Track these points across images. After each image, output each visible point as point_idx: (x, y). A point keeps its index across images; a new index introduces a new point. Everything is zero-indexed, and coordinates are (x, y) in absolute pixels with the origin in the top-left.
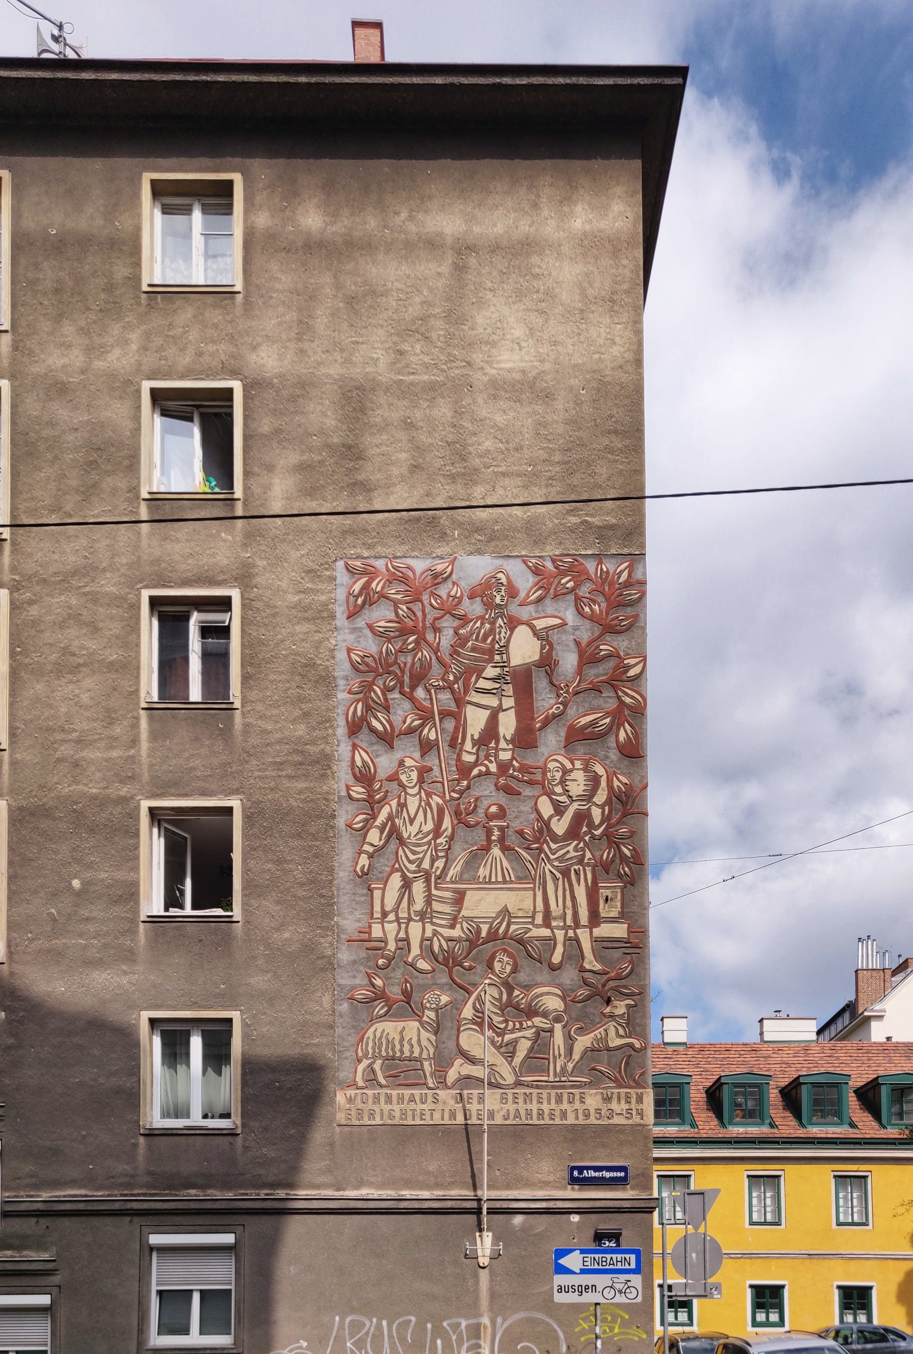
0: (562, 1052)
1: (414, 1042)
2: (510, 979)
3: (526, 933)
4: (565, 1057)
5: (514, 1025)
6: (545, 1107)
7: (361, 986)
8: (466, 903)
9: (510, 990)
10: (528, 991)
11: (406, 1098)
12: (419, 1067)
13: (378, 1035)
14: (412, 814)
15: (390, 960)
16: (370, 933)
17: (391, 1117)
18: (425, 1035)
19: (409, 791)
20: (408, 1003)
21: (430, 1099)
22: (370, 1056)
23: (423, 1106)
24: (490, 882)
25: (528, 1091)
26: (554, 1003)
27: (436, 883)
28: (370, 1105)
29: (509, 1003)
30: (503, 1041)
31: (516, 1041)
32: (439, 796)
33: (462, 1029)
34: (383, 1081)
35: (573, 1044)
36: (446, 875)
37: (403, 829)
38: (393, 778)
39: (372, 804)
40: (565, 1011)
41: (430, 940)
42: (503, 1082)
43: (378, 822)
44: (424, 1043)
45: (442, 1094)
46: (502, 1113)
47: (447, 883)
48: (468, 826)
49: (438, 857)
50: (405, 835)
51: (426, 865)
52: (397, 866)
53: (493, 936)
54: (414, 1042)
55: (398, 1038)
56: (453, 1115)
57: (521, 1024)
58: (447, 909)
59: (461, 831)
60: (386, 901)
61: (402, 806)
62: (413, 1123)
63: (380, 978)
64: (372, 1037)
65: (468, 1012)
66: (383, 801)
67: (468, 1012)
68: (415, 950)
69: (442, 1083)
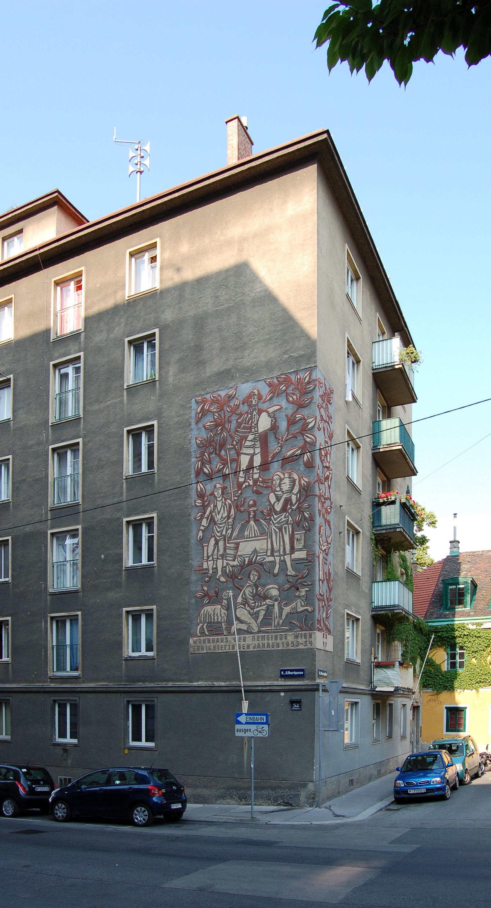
3: (263, 560)
6: (270, 642)
9: (257, 587)
11: (216, 640)
15: (210, 578)
16: (202, 566)
17: (210, 649)
18: (223, 611)
19: (219, 499)
21: (225, 640)
24: (249, 538)
26: (275, 592)
27: (228, 541)
38: (212, 494)
39: (204, 507)
40: (279, 596)
41: (226, 567)
43: (206, 516)
44: (223, 615)
46: (253, 645)
49: (229, 528)
51: (224, 533)
53: (250, 563)
54: (219, 614)
55: (212, 613)
58: (232, 552)
61: (215, 506)
65: (240, 600)
66: (208, 505)
67: (240, 600)
68: (220, 573)
69: (230, 633)
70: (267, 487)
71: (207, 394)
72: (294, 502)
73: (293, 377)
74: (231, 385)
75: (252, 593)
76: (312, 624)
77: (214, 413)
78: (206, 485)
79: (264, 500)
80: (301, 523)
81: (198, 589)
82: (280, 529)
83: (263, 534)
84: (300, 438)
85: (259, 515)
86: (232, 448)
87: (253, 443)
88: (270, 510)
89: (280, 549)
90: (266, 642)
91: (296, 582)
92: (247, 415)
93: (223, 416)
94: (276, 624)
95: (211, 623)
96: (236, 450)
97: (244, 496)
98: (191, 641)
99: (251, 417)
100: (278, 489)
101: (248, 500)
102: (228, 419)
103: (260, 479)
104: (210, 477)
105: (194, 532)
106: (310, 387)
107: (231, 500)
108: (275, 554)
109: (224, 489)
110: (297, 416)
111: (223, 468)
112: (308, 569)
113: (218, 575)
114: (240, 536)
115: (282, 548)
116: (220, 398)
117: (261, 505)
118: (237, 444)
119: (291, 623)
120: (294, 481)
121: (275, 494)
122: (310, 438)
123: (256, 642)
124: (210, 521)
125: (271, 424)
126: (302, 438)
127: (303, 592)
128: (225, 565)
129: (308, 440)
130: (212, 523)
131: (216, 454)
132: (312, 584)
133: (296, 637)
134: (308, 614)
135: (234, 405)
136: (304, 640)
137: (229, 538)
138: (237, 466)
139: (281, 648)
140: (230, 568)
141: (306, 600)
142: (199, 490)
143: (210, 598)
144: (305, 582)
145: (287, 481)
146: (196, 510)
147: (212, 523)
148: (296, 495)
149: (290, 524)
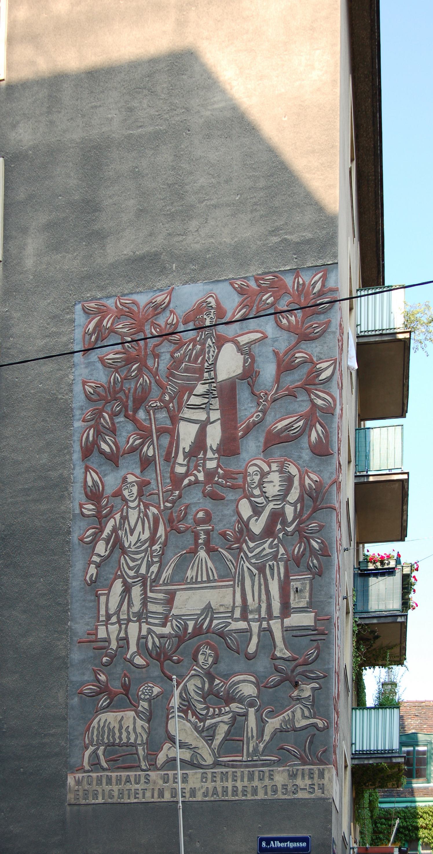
0: (255, 734)
2: (211, 670)
3: (226, 626)
4: (257, 739)
7: (88, 681)
8: (176, 603)
10: (227, 679)
11: (124, 779)
12: (135, 752)
13: (102, 724)
14: (132, 524)
15: (112, 657)
16: (96, 634)
17: (111, 796)
18: (140, 723)
19: (131, 505)
20: (127, 695)
21: (143, 780)
22: (95, 743)
23: (137, 786)
24: (196, 582)
25: (224, 770)
26: (249, 690)
27: (151, 586)
28: (95, 787)
29: (210, 692)
30: (204, 725)
32: (155, 507)
33: (170, 716)
34: (105, 765)
35: (264, 726)
37: (125, 539)
38: (118, 494)
39: (100, 519)
40: (258, 697)
41: (146, 637)
43: (104, 536)
44: (139, 730)
45: (153, 775)
47: (161, 585)
49: (153, 563)
50: (126, 545)
51: (143, 570)
52: (119, 573)
53: (198, 631)
55: (117, 726)
56: (161, 794)
57: (220, 710)
58: (159, 609)
59: (173, 538)
61: (125, 518)
62: (129, 801)
63: (104, 674)
64: (96, 726)
65: (175, 702)
66: (110, 515)
67: (175, 702)
68: (133, 648)
69: (153, 766)
70: (233, 487)
71: (108, 297)
72: (290, 518)
73: (289, 280)
74: (159, 285)
75: (202, 689)
76: (324, 752)
78: (105, 475)
79: (229, 511)
80: (303, 560)
81: (86, 678)
82: (261, 569)
83: (224, 577)
84: (302, 397)
85: (216, 541)
86: (161, 408)
87: (206, 401)
88: (241, 531)
89: (260, 606)
90: (229, 784)
91: (293, 671)
92: (194, 346)
94: (251, 749)
95: (113, 745)
96: (168, 411)
97: (186, 501)
98: (71, 780)
99: (202, 350)
100: (257, 492)
101: (194, 510)
102: (153, 351)
103: (219, 470)
104: (113, 459)
105: (79, 565)
107: (158, 508)
108: (250, 617)
109: (143, 485)
110: (297, 355)
111: (142, 444)
112: (317, 648)
114: (177, 578)
115: (264, 606)
116: (135, 308)
117: (220, 521)
119: (282, 748)
120: (289, 480)
121: (250, 501)
122: (324, 399)
123: (210, 785)
125: (244, 366)
126: (306, 398)
127: (307, 690)
129: (319, 402)
130: (117, 551)
131: (126, 416)
132: (325, 677)
133: (293, 776)
134: (317, 732)
135: (167, 324)
136: (308, 782)
137: (154, 581)
138: (171, 444)
139: (261, 796)
140: (156, 640)
141: (312, 706)
142: (90, 483)
143: (112, 696)
144: (312, 672)
145: (275, 477)
146: (82, 524)
147: (117, 551)
148: (294, 505)
149: (281, 559)
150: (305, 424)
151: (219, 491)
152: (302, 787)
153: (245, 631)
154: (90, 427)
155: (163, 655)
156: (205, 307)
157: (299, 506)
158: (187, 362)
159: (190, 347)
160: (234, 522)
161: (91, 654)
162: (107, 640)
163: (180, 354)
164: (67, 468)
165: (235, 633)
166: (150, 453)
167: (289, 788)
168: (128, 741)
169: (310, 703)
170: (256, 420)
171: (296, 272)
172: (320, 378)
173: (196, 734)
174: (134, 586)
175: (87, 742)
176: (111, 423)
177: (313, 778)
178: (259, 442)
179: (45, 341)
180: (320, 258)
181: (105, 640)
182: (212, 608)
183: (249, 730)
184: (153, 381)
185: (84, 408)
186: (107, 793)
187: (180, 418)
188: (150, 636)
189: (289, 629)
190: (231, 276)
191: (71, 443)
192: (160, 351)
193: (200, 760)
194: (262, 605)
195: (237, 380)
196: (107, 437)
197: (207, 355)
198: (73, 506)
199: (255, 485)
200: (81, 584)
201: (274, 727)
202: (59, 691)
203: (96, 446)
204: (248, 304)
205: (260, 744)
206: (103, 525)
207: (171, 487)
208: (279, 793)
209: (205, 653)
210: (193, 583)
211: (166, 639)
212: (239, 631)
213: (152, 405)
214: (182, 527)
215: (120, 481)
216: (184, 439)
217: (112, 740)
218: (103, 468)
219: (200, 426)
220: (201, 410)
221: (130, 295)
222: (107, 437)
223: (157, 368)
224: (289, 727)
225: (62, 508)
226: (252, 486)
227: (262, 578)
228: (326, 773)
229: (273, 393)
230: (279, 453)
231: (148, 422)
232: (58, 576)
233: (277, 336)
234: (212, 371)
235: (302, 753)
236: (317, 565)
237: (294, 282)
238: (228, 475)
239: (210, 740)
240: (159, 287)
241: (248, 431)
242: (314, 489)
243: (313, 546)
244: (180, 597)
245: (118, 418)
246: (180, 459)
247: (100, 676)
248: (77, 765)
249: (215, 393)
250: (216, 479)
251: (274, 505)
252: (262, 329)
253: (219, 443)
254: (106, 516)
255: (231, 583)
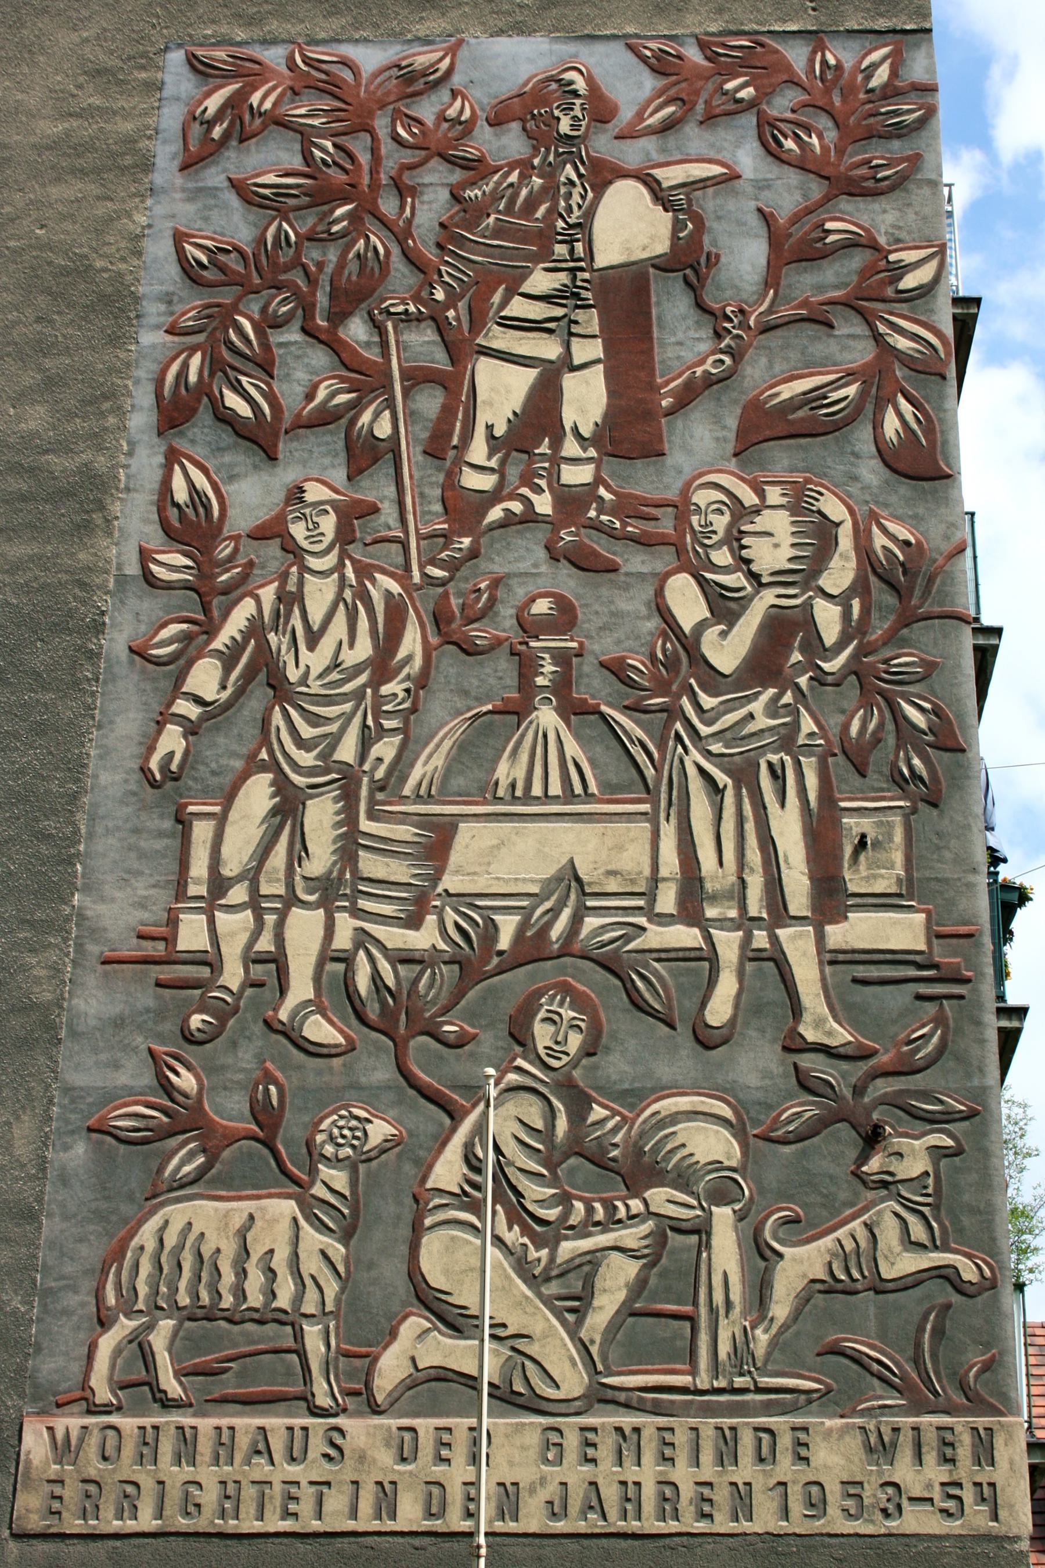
0: (736, 1295)
1: (280, 1262)
3: (627, 939)
4: (744, 1314)
5: (590, 1210)
6: (683, 1474)
7: (130, 1091)
8: (455, 857)
9: (579, 1103)
10: (631, 1107)
11: (243, 1442)
12: (290, 1343)
14: (316, 617)
15: (224, 1013)
16: (170, 939)
17: (190, 1506)
18: (312, 1239)
22: (140, 1305)
23: (293, 1471)
24: (528, 798)
25: (628, 1420)
26: (711, 1145)
27: (372, 802)
28: (127, 1467)
29: (576, 1147)
30: (552, 1259)
31: (592, 1261)
33: (428, 1222)
34: (172, 1386)
36: (403, 779)
38: (272, 531)
39: (206, 598)
41: (347, 959)
42: (550, 1392)
43: (219, 643)
44: (311, 1265)
45: (358, 1429)
46: (544, 1494)
47: (403, 799)
48: (469, 650)
49: (382, 732)
50: (293, 674)
51: (347, 752)
52: (264, 755)
53: (532, 948)
54: (280, 1262)
55: (229, 1248)
57: (611, 1209)
58: (399, 871)
60: (226, 850)
61: (291, 599)
62: (257, 1526)
63: (189, 1068)
64: (151, 1245)
65: (448, 1171)
67: (448, 1171)
68: (301, 988)
70: (644, 542)
71: (268, 42)
72: (830, 633)
73: (797, 55)
76: (987, 1367)
77: (305, 137)
78: (232, 478)
81: (123, 1078)
82: (745, 775)
84: (849, 326)
85: (593, 686)
86: (419, 318)
87: (559, 312)
90: (647, 1473)
91: (858, 1091)
92: (524, 177)
93: (364, 159)
94: (724, 1348)
96: (441, 326)
101: (521, 592)
103: (602, 491)
104: (260, 439)
105: (126, 723)
106: (896, 113)
107: (403, 576)
108: (711, 912)
109: (353, 516)
110: (829, 225)
111: (356, 407)
112: (940, 1021)
113: (291, 1001)
114: (458, 782)
115: (756, 884)
116: (347, 75)
118: (452, 301)
120: (821, 536)
121: (702, 582)
122: (915, 337)
124: (249, 675)
126: (860, 329)
127: (912, 1155)
128: (343, 940)
129: (903, 343)
132: (971, 1115)
133: (881, 1449)
134: (955, 1298)
135: (442, 117)
138: (448, 412)
139: (765, 1519)
142: (181, 494)
144: (926, 1095)
145: (779, 522)
146: (151, 606)
147: (259, 696)
148: (843, 600)
150: (863, 394)
151: (601, 546)
152: (917, 1493)
153: (693, 954)
154: (192, 350)
155: (403, 1017)
156: (556, 91)
157: (856, 604)
158: (499, 212)
159: (514, 177)
160: (651, 634)
161: (147, 998)
162: (210, 958)
163: (479, 193)
164: (107, 449)
165: (658, 960)
166: (383, 429)
167: (867, 1494)
168: (267, 1304)
169: (929, 1200)
170: (714, 371)
171: (816, 38)
172: (902, 286)
173: (524, 1287)
174: (312, 797)
175: (111, 1300)
176: (260, 345)
177: (952, 1461)
178: (724, 427)
179: (66, 125)
180: (881, 15)
181: (198, 959)
182: (578, 880)
183: (717, 1280)
184: (396, 251)
185: (175, 299)
186: (174, 1495)
187: (477, 348)
188: (361, 953)
189: (841, 957)
190: (630, 30)
191: (126, 386)
192: (420, 181)
193: (536, 1380)
194: (749, 879)
195: (651, 270)
196: (244, 379)
197: (563, 203)
198: (119, 555)
199: (715, 538)
200: (126, 781)
201: (804, 1276)
202: (18, 1118)
203: (205, 399)
204: (683, 96)
205: (758, 1332)
206: (216, 613)
207: (446, 526)
208: (833, 1511)
209: (556, 1017)
210: (515, 800)
211: (418, 968)
212: (672, 955)
213: (392, 310)
214: (480, 634)
215: (280, 496)
216: (490, 404)
217: (205, 1298)
218: (227, 458)
219: (541, 374)
220: (545, 335)
221: (334, 45)
222: (244, 379)
223: (409, 222)
224: (856, 1275)
225: (81, 556)
226: (707, 542)
227: (746, 801)
228: (999, 1442)
229: (762, 309)
230: (786, 462)
231: (377, 350)
232: (51, 753)
233: (769, 176)
234: (578, 240)
235: (909, 1368)
236: (925, 774)
237: (811, 61)
238: (628, 507)
239: (572, 1310)
240: (421, 34)
241: (688, 395)
242: (902, 564)
243: (906, 718)
244: (471, 842)
245: (282, 333)
246: (478, 451)
247: (177, 1074)
248: (64, 1386)
249: (584, 294)
250: (592, 514)
251: (779, 596)
252: (725, 156)
253: (599, 421)
254: (226, 590)
255: (645, 807)
